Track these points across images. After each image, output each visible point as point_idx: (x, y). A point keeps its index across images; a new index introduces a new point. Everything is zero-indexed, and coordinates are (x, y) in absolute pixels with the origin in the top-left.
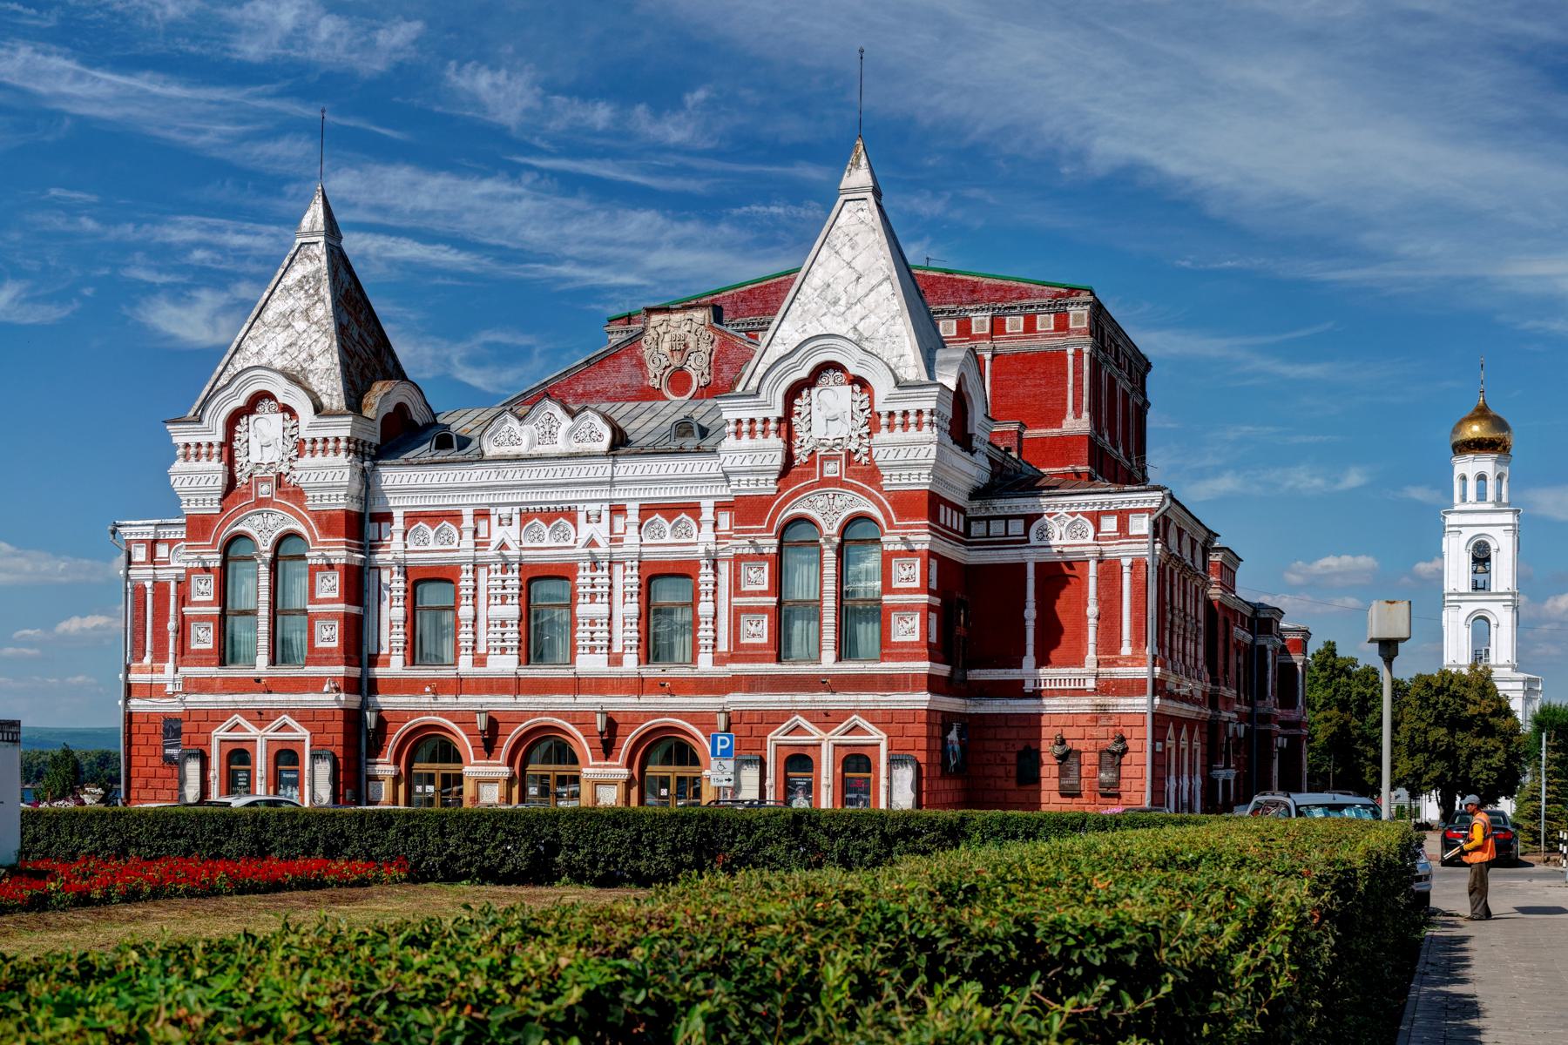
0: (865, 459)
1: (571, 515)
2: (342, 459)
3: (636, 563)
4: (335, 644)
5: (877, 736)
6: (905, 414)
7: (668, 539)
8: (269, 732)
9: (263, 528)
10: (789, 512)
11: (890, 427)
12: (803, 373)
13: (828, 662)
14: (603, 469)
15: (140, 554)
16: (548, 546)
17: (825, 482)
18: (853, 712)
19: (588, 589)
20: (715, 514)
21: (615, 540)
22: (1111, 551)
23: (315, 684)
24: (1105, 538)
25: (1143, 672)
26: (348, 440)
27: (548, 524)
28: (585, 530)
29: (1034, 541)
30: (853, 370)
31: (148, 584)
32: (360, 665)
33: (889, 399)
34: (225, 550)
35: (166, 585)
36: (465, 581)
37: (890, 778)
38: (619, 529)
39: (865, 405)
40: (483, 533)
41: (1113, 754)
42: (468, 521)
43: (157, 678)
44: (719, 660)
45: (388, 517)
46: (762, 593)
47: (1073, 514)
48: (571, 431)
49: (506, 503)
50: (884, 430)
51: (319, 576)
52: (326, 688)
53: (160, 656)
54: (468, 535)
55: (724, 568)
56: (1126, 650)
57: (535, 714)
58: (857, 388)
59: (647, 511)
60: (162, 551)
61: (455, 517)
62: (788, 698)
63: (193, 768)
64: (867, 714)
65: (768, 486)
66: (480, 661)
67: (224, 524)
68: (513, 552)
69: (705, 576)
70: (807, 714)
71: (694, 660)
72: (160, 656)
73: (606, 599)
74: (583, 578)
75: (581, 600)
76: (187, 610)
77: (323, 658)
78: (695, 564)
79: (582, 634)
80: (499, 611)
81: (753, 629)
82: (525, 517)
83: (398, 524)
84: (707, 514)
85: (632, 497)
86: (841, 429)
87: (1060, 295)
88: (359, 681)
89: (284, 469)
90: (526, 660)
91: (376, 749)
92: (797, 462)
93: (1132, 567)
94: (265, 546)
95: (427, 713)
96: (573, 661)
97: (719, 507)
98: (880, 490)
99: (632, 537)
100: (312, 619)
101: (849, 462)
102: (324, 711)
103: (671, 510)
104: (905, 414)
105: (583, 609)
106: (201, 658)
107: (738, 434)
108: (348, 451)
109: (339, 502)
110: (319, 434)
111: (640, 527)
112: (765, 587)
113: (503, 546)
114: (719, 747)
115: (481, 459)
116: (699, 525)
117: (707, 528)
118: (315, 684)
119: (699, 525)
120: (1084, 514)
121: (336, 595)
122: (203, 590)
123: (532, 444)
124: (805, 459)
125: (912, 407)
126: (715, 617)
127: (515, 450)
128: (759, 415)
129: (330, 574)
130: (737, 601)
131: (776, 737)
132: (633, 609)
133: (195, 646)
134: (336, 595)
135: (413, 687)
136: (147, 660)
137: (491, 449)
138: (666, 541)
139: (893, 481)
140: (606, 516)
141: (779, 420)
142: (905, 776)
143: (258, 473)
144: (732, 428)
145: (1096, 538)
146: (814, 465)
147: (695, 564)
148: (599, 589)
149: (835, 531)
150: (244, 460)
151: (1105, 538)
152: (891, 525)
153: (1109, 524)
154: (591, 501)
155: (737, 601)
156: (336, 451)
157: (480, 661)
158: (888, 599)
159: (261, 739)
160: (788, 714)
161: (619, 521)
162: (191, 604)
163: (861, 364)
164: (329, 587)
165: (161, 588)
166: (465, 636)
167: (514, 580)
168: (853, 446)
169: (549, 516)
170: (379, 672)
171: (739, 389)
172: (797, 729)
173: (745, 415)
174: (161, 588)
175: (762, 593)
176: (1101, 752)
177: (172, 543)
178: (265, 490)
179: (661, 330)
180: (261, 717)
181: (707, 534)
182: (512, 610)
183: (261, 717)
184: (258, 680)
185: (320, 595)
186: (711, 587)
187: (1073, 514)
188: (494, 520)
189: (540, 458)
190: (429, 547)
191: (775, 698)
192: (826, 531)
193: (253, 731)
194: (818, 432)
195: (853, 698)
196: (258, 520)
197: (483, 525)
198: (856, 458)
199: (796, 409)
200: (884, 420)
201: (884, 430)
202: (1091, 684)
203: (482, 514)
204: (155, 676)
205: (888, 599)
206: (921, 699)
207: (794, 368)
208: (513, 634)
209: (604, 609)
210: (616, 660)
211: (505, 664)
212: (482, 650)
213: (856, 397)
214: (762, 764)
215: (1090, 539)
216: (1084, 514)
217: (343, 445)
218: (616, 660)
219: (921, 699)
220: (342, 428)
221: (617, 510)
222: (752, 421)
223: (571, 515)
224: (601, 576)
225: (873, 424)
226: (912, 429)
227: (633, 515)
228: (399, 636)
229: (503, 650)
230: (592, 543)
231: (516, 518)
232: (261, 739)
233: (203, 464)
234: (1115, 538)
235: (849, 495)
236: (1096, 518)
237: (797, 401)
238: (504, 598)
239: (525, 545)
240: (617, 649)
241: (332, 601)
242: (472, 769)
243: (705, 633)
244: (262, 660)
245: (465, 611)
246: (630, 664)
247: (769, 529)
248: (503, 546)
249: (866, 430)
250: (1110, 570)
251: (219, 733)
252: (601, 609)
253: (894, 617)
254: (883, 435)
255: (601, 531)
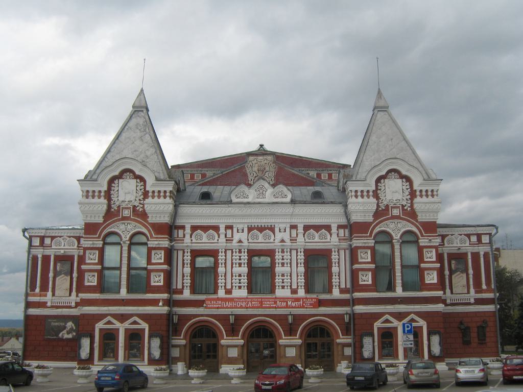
0: (409, 209)
1: (272, 229)
2: (168, 200)
3: (302, 250)
4: (162, 284)
5: (422, 323)
6: (427, 191)
7: (317, 239)
8: (127, 325)
9: (125, 230)
10: (377, 229)
11: (421, 196)
12: (384, 173)
13: (399, 292)
14: (289, 209)
15: (36, 242)
16: (261, 241)
17: (394, 217)
18: (411, 313)
19: (281, 261)
20: (338, 230)
21: (293, 240)
22: (476, 249)
23: (154, 302)
24: (472, 244)
25: (490, 295)
26: (171, 192)
27: (261, 232)
28: (279, 236)
29: (446, 245)
30: (404, 173)
31: (40, 256)
32: (169, 293)
33: (420, 185)
34: (104, 240)
35: (49, 257)
36: (221, 257)
37: (429, 340)
38: (294, 235)
39: (408, 187)
40: (229, 235)
41: (483, 327)
42: (222, 230)
43: (43, 299)
44: (342, 291)
45: (183, 227)
46: (368, 263)
47: (461, 235)
48: (273, 192)
49: (240, 223)
50: (418, 197)
51: (153, 252)
52: (161, 304)
53: (44, 288)
54: (222, 236)
55: (342, 252)
56: (484, 287)
57: (256, 316)
58: (404, 180)
59: (307, 228)
60: (47, 241)
61: (216, 228)
62: (384, 307)
63: (85, 342)
64: (418, 314)
65: (370, 218)
66: (229, 292)
67: (105, 228)
68: (245, 243)
69: (334, 257)
70: (392, 314)
71: (330, 292)
72: (44, 288)
73: (289, 265)
74: (278, 256)
75: (277, 265)
76: (83, 267)
77: (157, 290)
78: (330, 251)
79: (278, 280)
80: (237, 270)
81: (364, 278)
82: (250, 229)
83: (188, 230)
84: (334, 230)
85: (301, 222)
86: (399, 196)
87: (339, 167)
88: (170, 300)
89: (136, 204)
90: (250, 290)
91: (176, 332)
92: (380, 209)
93: (484, 255)
94: (126, 237)
95: (202, 315)
96: (273, 291)
97: (339, 227)
98: (417, 221)
99: (301, 239)
100: (149, 272)
101: (403, 209)
102: (161, 315)
103: (317, 228)
104: (427, 191)
105: (278, 269)
106: (90, 289)
107: (356, 197)
108: (170, 197)
109: (166, 219)
110: (156, 189)
111: (304, 235)
112: (369, 260)
113: (240, 241)
114: (406, 329)
115: (230, 202)
116: (331, 235)
117: (334, 236)
118: (154, 302)
119: (331, 235)
120: (464, 235)
121: (162, 261)
122: (92, 258)
123: (254, 198)
124: (384, 208)
125: (430, 189)
126: (339, 273)
127: (245, 200)
128: (365, 189)
129: (158, 252)
130: (356, 266)
131: (378, 324)
132: (302, 269)
133: (87, 284)
134: (162, 261)
135: (199, 304)
136: (37, 290)
137: (234, 200)
138: (317, 241)
139: (422, 218)
140: (288, 230)
141: (373, 191)
142: (436, 339)
143: (124, 205)
144: (353, 194)
145: (470, 244)
146: (388, 210)
147: (330, 251)
148: (285, 261)
149: (399, 237)
150: (116, 199)
151: (472, 244)
152: (422, 235)
153: (474, 239)
154: (281, 222)
155: (356, 266)
156: (165, 197)
157: (229, 292)
158: (423, 265)
159: (122, 328)
160: (382, 314)
161: (294, 232)
162: (86, 264)
163: (408, 170)
164: (159, 257)
165: (46, 259)
166: (221, 281)
167: (245, 256)
168: (404, 203)
169: (261, 229)
170: (177, 297)
171: (354, 178)
172: (387, 321)
173: (359, 189)
174: (46, 259)
175: (368, 263)
176: (478, 327)
177: (53, 238)
178: (126, 213)
179: (254, 162)
180: (122, 318)
181: (335, 239)
182: (244, 270)
183: (122, 318)
184: (123, 300)
185: (153, 261)
186: (337, 260)
187: (461, 235)
188: (235, 230)
189: (259, 203)
190: (204, 241)
191: (378, 307)
192: (395, 238)
193: (117, 324)
194: (389, 197)
195: (412, 307)
196: (122, 227)
197: (229, 232)
198: (405, 208)
199: (379, 188)
200: (418, 193)
201: (418, 197)
202: (472, 301)
203: (229, 227)
204: (42, 298)
205: (423, 265)
206: (440, 307)
207: (380, 170)
208: (244, 280)
209: (289, 269)
210: (294, 292)
211: (243, 293)
212: (229, 287)
213: (404, 184)
214: (372, 335)
215: (468, 244)
216: (464, 235)
217: (168, 194)
218: (294, 292)
219: (440, 307)
220: (169, 187)
221: (294, 227)
222: (362, 191)
223: (272, 229)
224: (287, 255)
225: (413, 194)
226: (430, 197)
227: (301, 230)
228: (188, 281)
229: (240, 287)
230: (283, 241)
231: (246, 230)
232: (122, 328)
233: (96, 200)
234: (476, 244)
235: (404, 222)
236: (468, 236)
237: (379, 184)
238: (240, 265)
239: (250, 241)
240: (294, 287)
241: (160, 264)
242: (283, 341)
243: (335, 280)
244: (124, 291)
245: (221, 270)
246: (301, 293)
247: (370, 236)
248: (240, 241)
249: (409, 197)
250: (476, 256)
251: (100, 325)
252: (286, 269)
253: (426, 272)
254: (418, 199)
255: (286, 236)
